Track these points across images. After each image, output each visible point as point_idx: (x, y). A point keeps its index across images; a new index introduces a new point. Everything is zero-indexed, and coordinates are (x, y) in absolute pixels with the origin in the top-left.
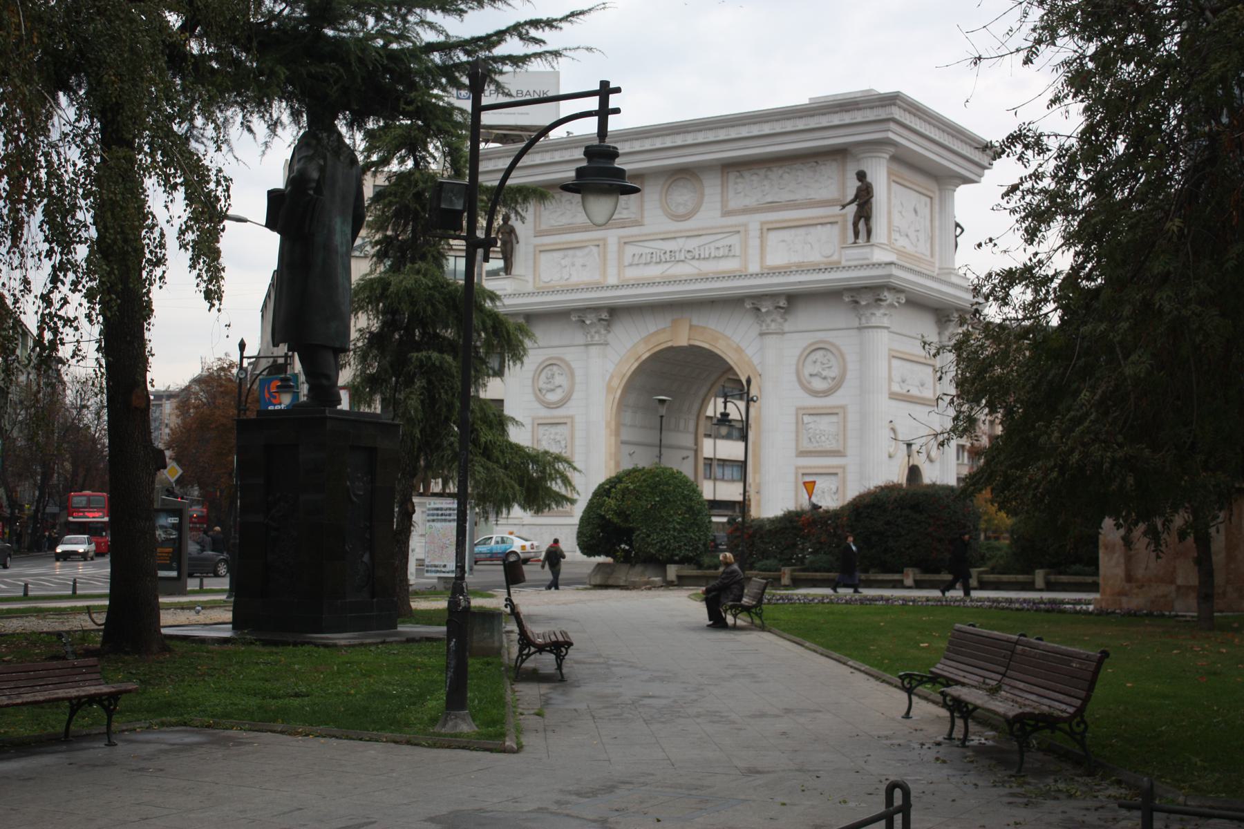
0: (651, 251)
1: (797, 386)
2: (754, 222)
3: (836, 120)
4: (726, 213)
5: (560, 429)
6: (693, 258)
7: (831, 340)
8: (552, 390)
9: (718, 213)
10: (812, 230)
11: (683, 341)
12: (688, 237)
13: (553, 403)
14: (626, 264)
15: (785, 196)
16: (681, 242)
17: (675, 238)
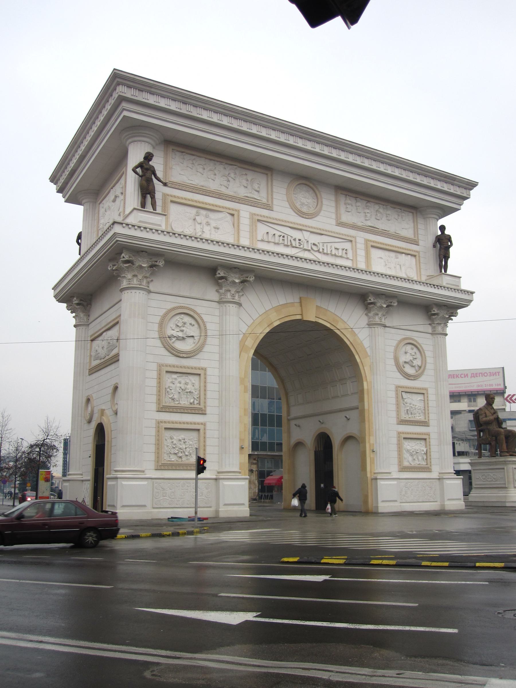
0: (283, 235)
1: (395, 369)
2: (361, 237)
3: (439, 185)
4: (340, 224)
5: (194, 379)
6: (318, 251)
7: (415, 338)
8: (183, 338)
9: (334, 222)
10: (399, 255)
11: (311, 316)
12: (311, 232)
13: (183, 352)
14: (260, 238)
15: (381, 225)
16: (306, 234)
17: (301, 230)
